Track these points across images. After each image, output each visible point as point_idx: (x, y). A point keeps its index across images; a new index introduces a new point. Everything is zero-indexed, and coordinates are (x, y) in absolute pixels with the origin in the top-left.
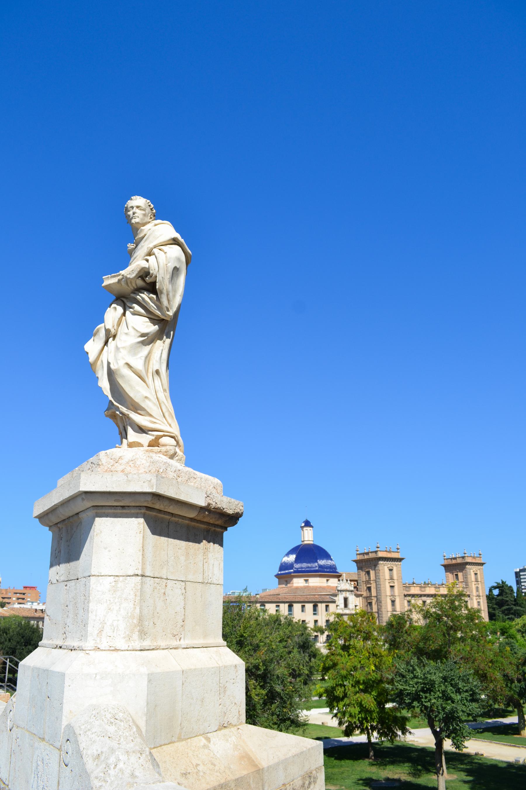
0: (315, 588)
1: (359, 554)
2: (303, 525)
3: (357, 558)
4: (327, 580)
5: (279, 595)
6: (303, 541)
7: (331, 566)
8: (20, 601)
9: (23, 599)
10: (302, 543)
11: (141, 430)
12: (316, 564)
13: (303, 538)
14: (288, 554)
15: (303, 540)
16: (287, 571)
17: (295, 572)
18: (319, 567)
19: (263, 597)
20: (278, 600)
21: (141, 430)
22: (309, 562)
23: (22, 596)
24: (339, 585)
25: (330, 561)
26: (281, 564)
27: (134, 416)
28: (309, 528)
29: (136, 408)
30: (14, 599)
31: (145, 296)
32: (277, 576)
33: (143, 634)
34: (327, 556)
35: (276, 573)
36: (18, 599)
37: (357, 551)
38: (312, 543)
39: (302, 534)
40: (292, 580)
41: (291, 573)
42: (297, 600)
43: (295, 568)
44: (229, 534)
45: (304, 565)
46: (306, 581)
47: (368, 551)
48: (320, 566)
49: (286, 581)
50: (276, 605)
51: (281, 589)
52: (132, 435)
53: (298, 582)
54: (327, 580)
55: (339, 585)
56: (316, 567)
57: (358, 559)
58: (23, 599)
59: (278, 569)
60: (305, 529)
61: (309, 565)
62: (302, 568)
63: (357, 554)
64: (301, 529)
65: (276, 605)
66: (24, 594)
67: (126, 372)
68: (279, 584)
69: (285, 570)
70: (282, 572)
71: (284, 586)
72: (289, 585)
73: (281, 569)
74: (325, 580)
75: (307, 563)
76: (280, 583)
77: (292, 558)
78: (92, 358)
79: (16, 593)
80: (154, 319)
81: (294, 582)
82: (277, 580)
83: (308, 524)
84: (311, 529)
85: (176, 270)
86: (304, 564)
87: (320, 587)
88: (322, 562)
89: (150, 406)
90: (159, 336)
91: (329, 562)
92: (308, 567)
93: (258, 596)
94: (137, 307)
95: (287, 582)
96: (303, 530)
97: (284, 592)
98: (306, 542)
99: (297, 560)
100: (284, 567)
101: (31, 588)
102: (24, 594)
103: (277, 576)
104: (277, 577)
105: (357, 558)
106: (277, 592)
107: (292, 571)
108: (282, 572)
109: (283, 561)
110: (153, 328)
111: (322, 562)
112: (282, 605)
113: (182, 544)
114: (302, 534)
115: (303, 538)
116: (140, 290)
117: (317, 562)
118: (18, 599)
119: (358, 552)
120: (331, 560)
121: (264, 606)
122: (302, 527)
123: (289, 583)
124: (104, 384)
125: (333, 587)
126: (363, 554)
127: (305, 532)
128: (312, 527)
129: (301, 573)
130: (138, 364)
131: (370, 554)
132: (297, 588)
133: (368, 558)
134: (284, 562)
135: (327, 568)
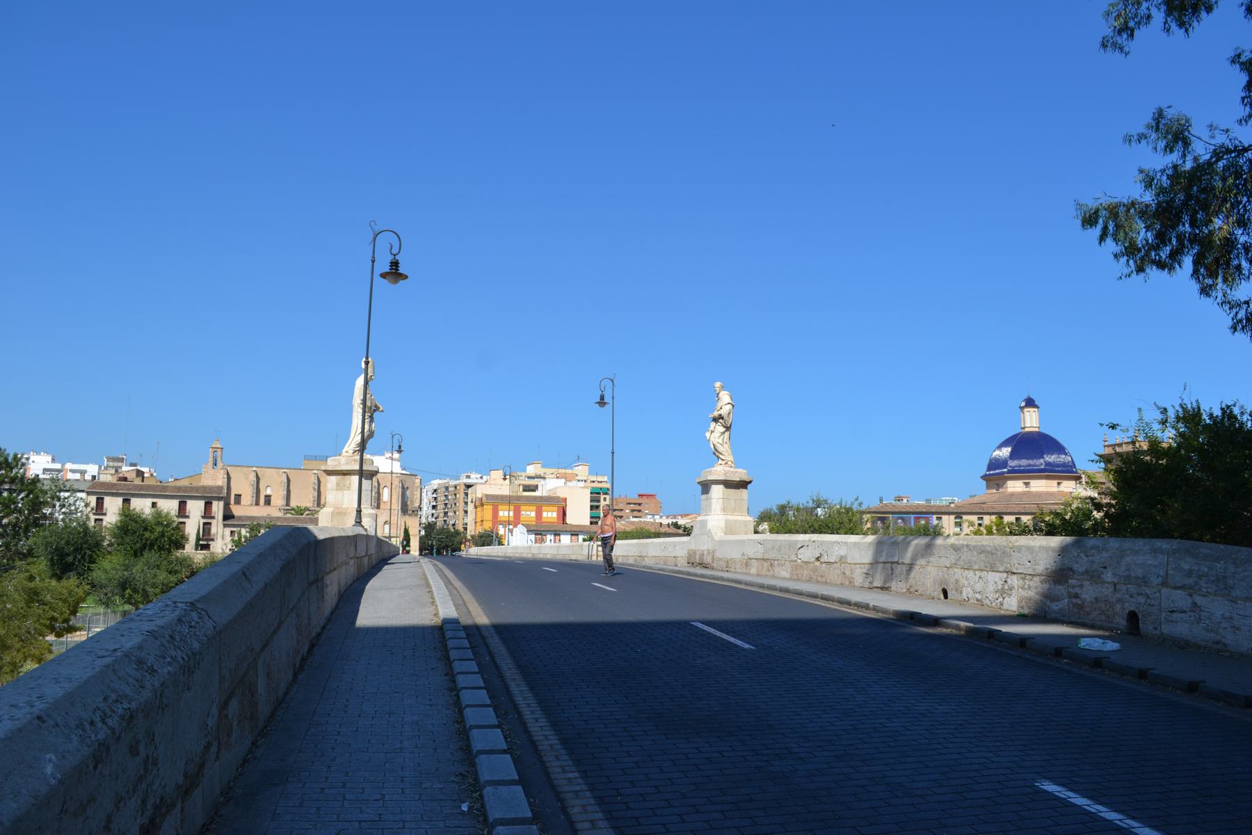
0: (1039, 495)
1: (1108, 446)
2: (1023, 404)
3: (1105, 451)
4: (1059, 484)
5: (985, 503)
6: (1024, 428)
7: (1064, 463)
8: (636, 514)
9: (639, 511)
10: (1023, 431)
11: (723, 460)
12: (1042, 461)
13: (1022, 423)
14: (1000, 447)
15: (1023, 426)
16: (997, 471)
17: (1009, 472)
18: (1046, 465)
19: (960, 507)
20: (981, 511)
21: (723, 460)
22: (1032, 458)
23: (637, 507)
24: (1074, 491)
25: (1063, 456)
26: (991, 461)
27: (721, 456)
28: (1032, 410)
29: (721, 454)
30: (628, 511)
31: (721, 421)
32: (984, 477)
33: (724, 511)
34: (1058, 448)
35: (983, 473)
36: (633, 511)
37: (1105, 441)
38: (1037, 430)
39: (1022, 417)
40: (1006, 482)
41: (1004, 473)
42: (1009, 511)
43: (1010, 467)
44: (749, 486)
45: (1024, 462)
46: (1027, 484)
47: (1121, 442)
48: (1048, 464)
49: (998, 485)
50: (979, 518)
51: (990, 496)
52: (720, 462)
53: (1015, 486)
54: (1059, 484)
55: (1074, 491)
56: (1042, 464)
57: (1107, 453)
58: (639, 511)
59: (986, 468)
60: (1026, 410)
61: (1031, 462)
62: (1020, 466)
63: (1105, 446)
64: (1020, 410)
65: (979, 518)
66: (640, 504)
67: (718, 445)
68: (988, 487)
69: (995, 469)
70: (992, 472)
71: (995, 491)
72: (1001, 490)
73: (989, 469)
74: (1055, 482)
75: (1028, 459)
76: (988, 487)
77: (1006, 451)
78: (708, 438)
79: (630, 504)
80: (724, 427)
81: (1008, 486)
82: (985, 482)
83: (1030, 403)
84: (1036, 410)
85: (729, 413)
86: (1023, 460)
87: (1048, 493)
88: (1051, 458)
89: (724, 453)
90: (726, 431)
91: (1062, 458)
92: (1029, 465)
93: (952, 505)
94: (719, 424)
95: (998, 486)
96: (1023, 412)
97: (993, 499)
98: (1027, 430)
99: (1013, 455)
100: (994, 464)
101: (648, 496)
102: (640, 504)
103: (984, 477)
104: (984, 480)
105: (1105, 451)
106: (983, 500)
107: (1006, 470)
108: (992, 472)
109: (993, 456)
110: (724, 429)
111: (1051, 458)
112: (945, 518)
113: (734, 490)
114: (1022, 417)
115: (1022, 423)
116: (720, 418)
117: (1043, 458)
118: (633, 511)
119: (1106, 443)
120: (1066, 454)
121: (961, 518)
122: (1022, 408)
123: (1002, 487)
124: (712, 446)
125: (1067, 493)
126: (1114, 446)
127: (1027, 414)
128: (1037, 407)
129: (1017, 473)
130: (721, 442)
131: (1124, 445)
132: (1012, 494)
133: (1121, 451)
134: (996, 459)
135: (1058, 466)
